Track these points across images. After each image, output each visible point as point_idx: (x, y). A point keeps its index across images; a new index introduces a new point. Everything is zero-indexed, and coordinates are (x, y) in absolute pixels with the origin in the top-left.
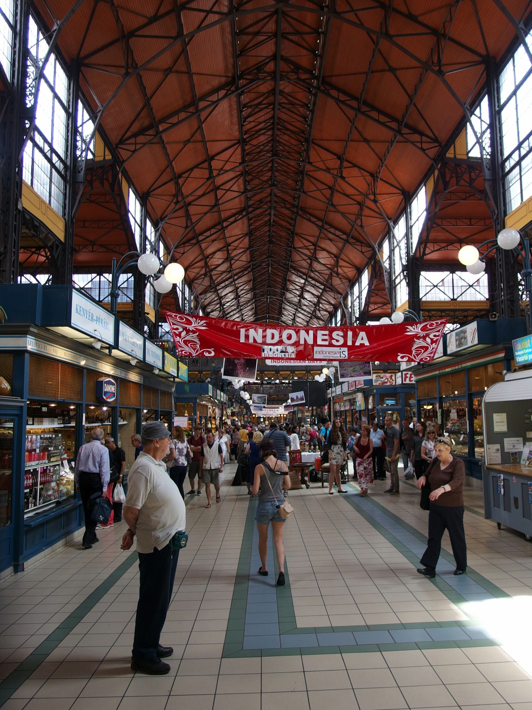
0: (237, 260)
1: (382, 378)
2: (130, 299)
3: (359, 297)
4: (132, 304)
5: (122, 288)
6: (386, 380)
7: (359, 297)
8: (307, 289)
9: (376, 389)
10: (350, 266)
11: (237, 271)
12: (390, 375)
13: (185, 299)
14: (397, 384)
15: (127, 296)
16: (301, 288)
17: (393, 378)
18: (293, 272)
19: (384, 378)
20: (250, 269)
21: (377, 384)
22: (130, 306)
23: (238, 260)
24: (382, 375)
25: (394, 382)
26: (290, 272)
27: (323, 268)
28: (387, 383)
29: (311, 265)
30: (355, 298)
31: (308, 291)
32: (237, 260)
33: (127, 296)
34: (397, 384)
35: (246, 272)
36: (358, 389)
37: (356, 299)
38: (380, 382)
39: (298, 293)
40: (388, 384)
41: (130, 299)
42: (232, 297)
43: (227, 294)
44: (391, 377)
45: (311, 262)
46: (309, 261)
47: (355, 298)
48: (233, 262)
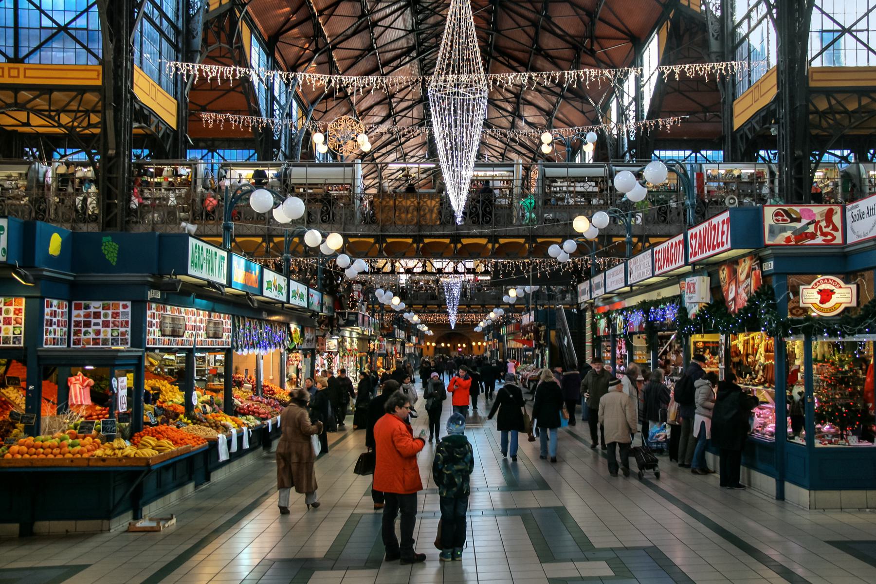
0: (387, 28)
1: (798, 220)
2: (96, 57)
3: (638, 98)
4: (100, 68)
5: (76, 29)
6: (811, 229)
7: (638, 98)
8: (529, 98)
9: (777, 258)
10: (620, 34)
11: (389, 55)
12: (824, 209)
13: (273, 98)
14: (851, 239)
15: (89, 51)
16: (517, 96)
17: (837, 219)
18: (501, 59)
19: (804, 222)
20: (414, 54)
21: (780, 239)
22: (94, 75)
23: (389, 27)
24: (797, 209)
25: (838, 235)
26: (495, 59)
27: (560, 44)
28: (813, 236)
29: (535, 40)
30: (626, 101)
31: (530, 103)
32: (387, 28)
33: (89, 51)
34: (851, 239)
35: (408, 59)
36: (694, 264)
37: (630, 104)
38: (789, 233)
39: (510, 109)
40: (819, 240)
41: (96, 57)
42: (384, 114)
43: (371, 107)
44: (829, 216)
45: (537, 33)
46: (531, 31)
47: (626, 103)
48: (377, 31)
